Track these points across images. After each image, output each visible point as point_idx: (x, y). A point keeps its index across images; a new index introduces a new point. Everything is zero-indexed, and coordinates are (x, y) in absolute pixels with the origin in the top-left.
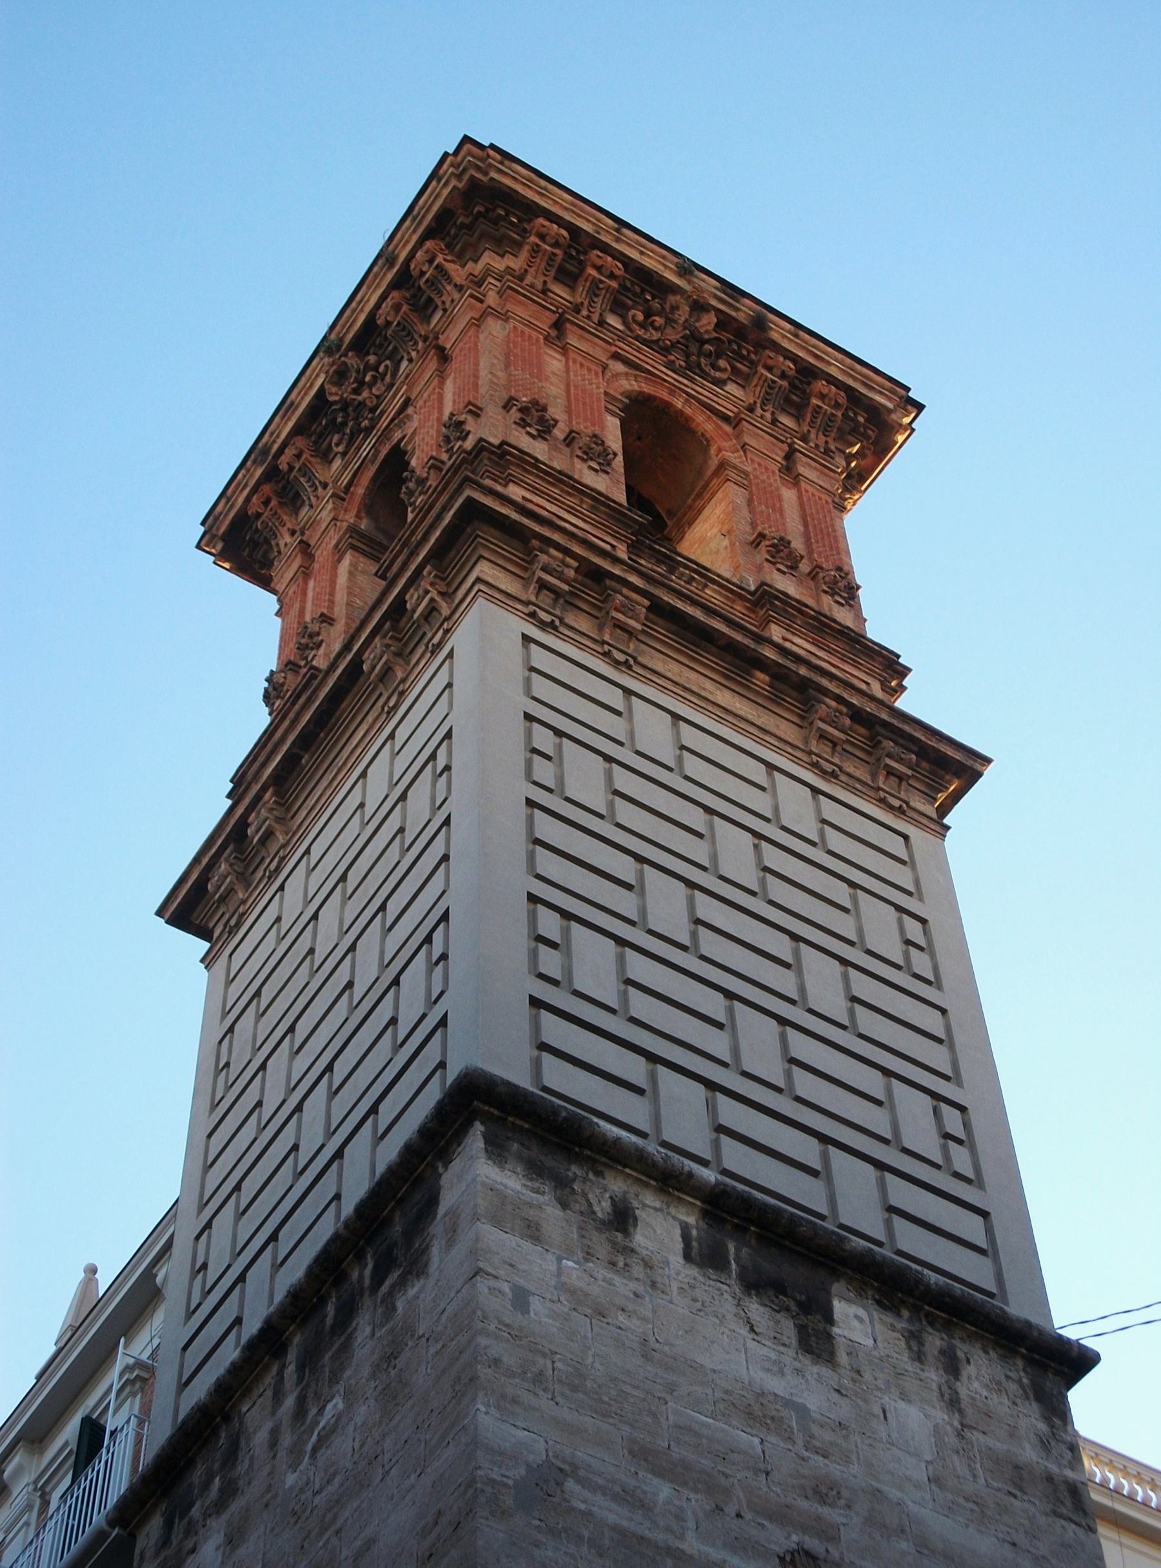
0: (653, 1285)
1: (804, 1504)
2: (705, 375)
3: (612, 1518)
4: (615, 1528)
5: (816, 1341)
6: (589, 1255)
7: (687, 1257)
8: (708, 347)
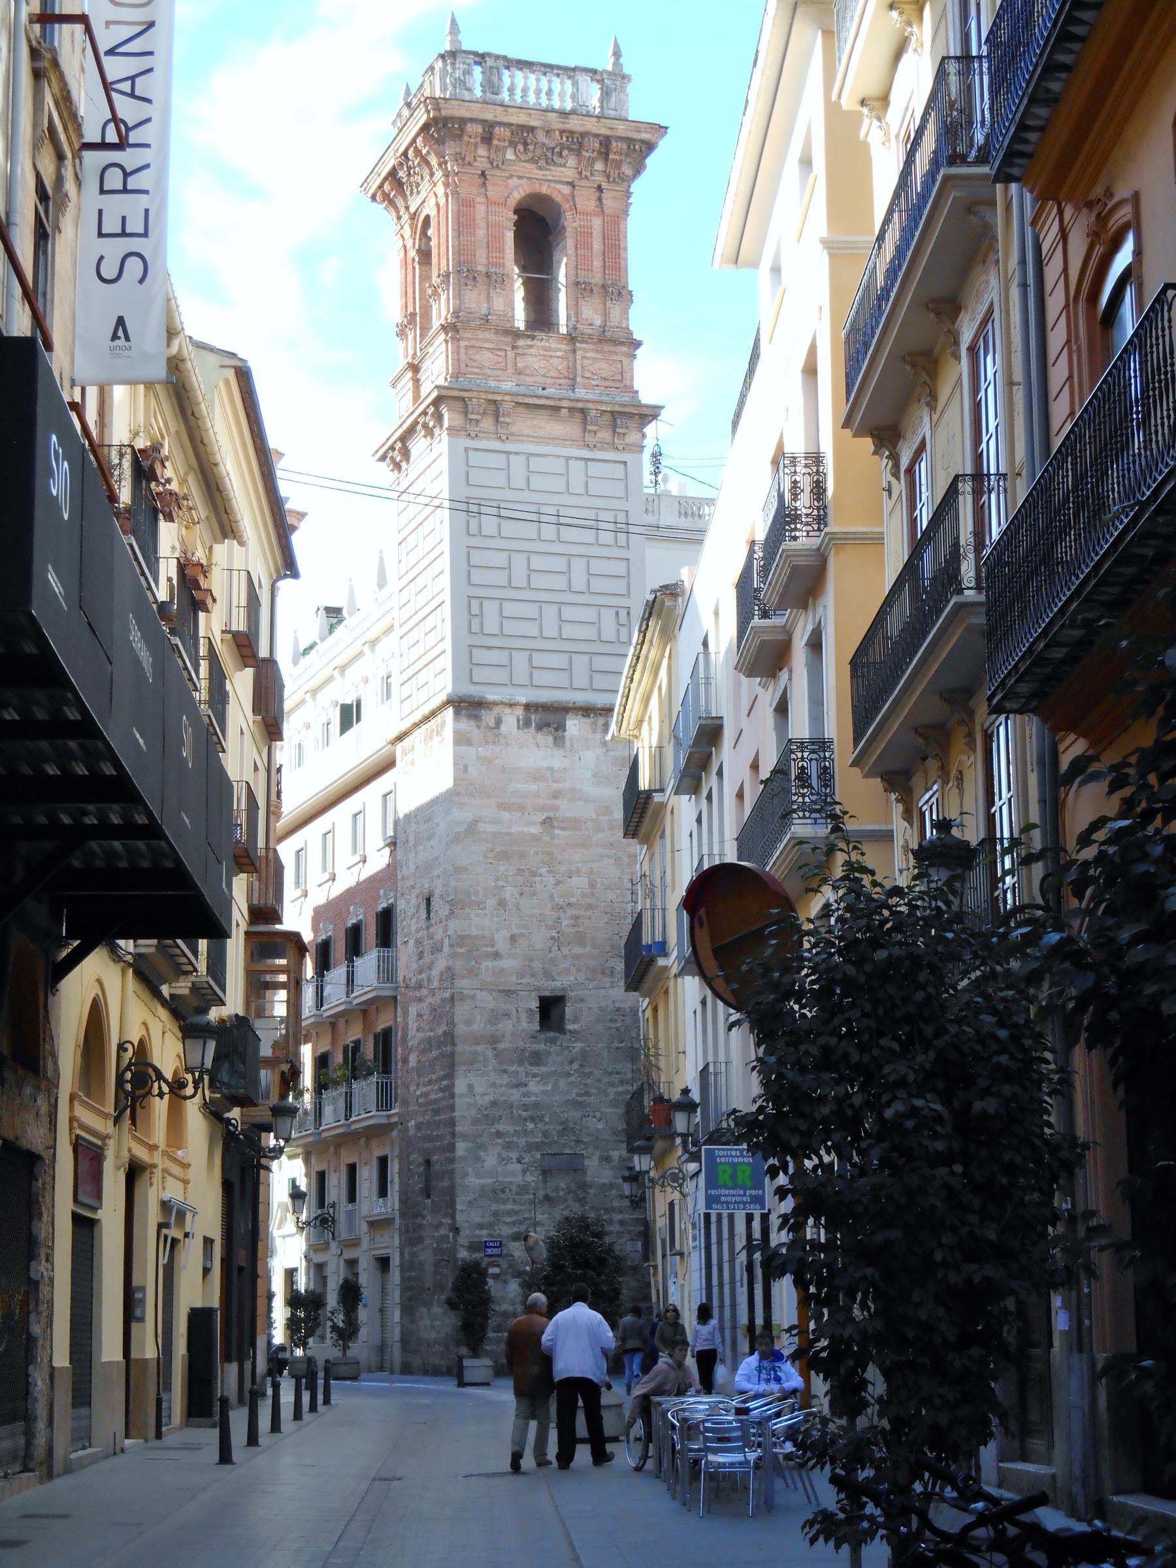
0: (507, 744)
1: (550, 802)
2: (555, 164)
3: (490, 830)
4: (493, 833)
5: (559, 741)
6: (487, 742)
7: (518, 728)
8: (557, 149)
